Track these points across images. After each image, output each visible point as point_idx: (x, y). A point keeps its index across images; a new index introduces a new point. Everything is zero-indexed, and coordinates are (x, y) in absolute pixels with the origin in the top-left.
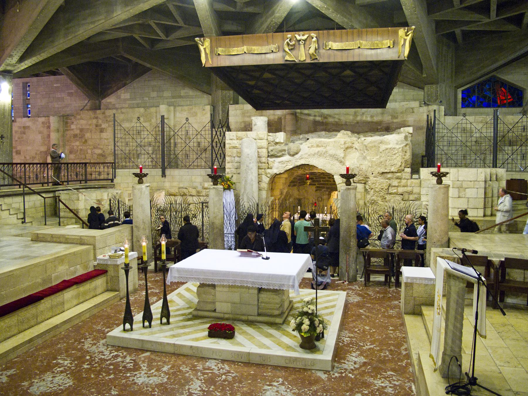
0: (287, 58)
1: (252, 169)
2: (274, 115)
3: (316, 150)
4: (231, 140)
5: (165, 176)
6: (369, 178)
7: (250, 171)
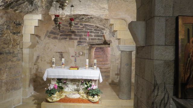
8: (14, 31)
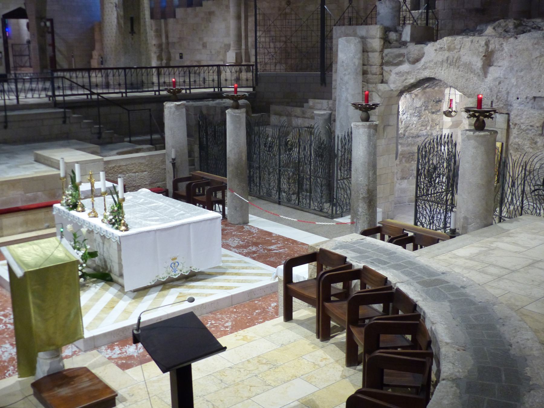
1: (347, 83)
5: (325, 84)
7: (344, 87)
8: (433, 110)
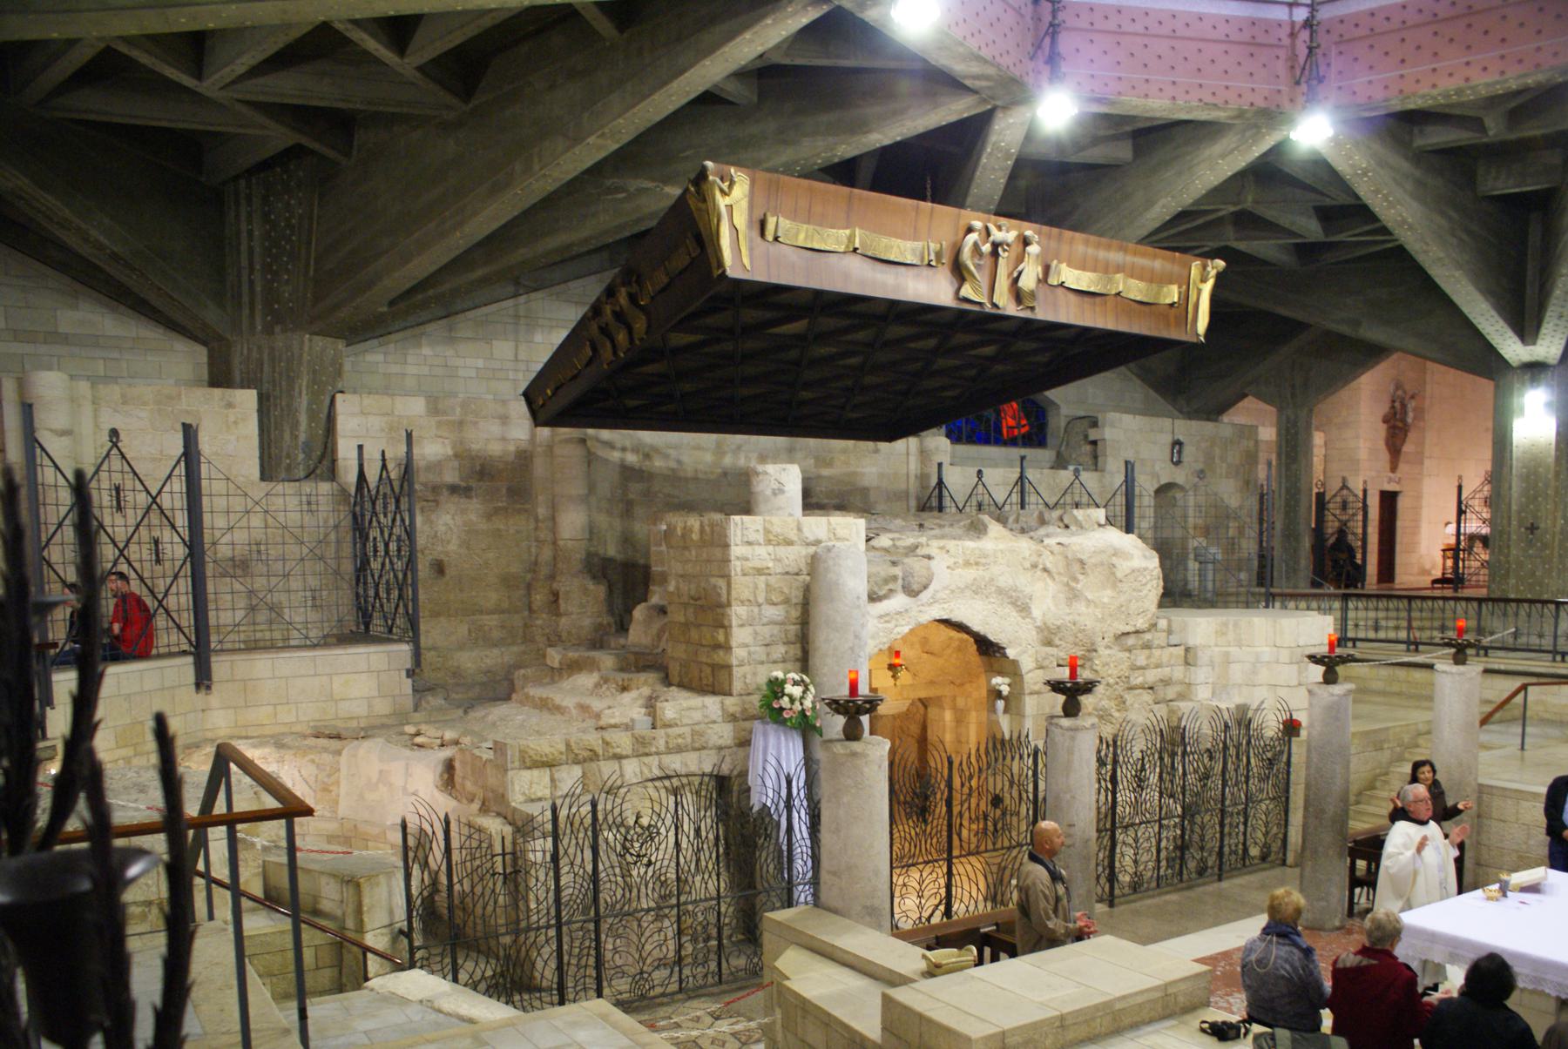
0: (967, 291)
2: (504, 439)
3: (971, 574)
4: (749, 543)
6: (1096, 651)
